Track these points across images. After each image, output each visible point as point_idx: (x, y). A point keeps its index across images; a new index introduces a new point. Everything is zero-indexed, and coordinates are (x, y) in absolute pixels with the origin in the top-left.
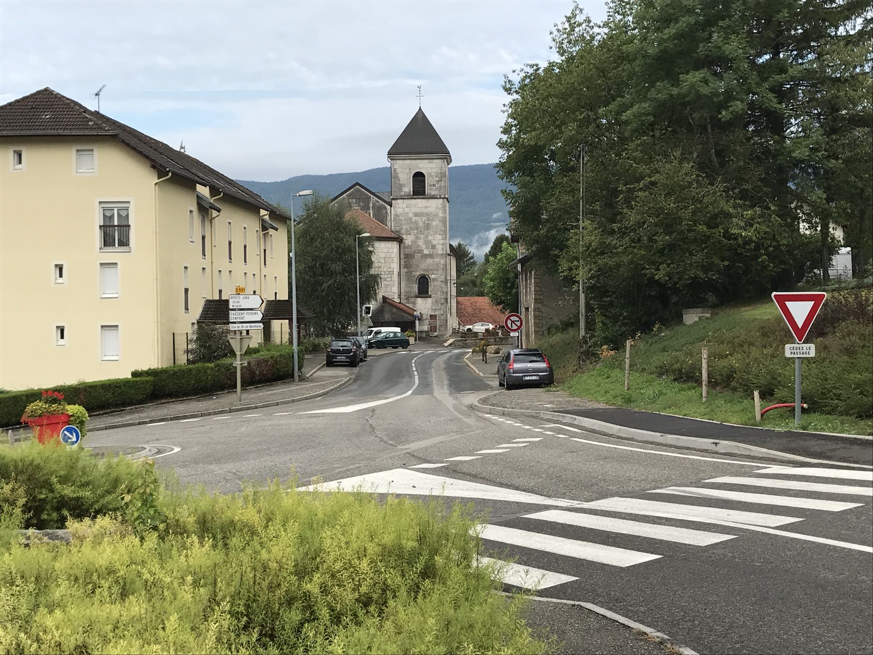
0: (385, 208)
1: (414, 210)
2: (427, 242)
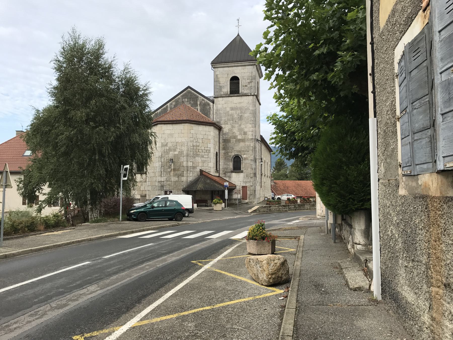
0: (209, 105)
2: (240, 130)
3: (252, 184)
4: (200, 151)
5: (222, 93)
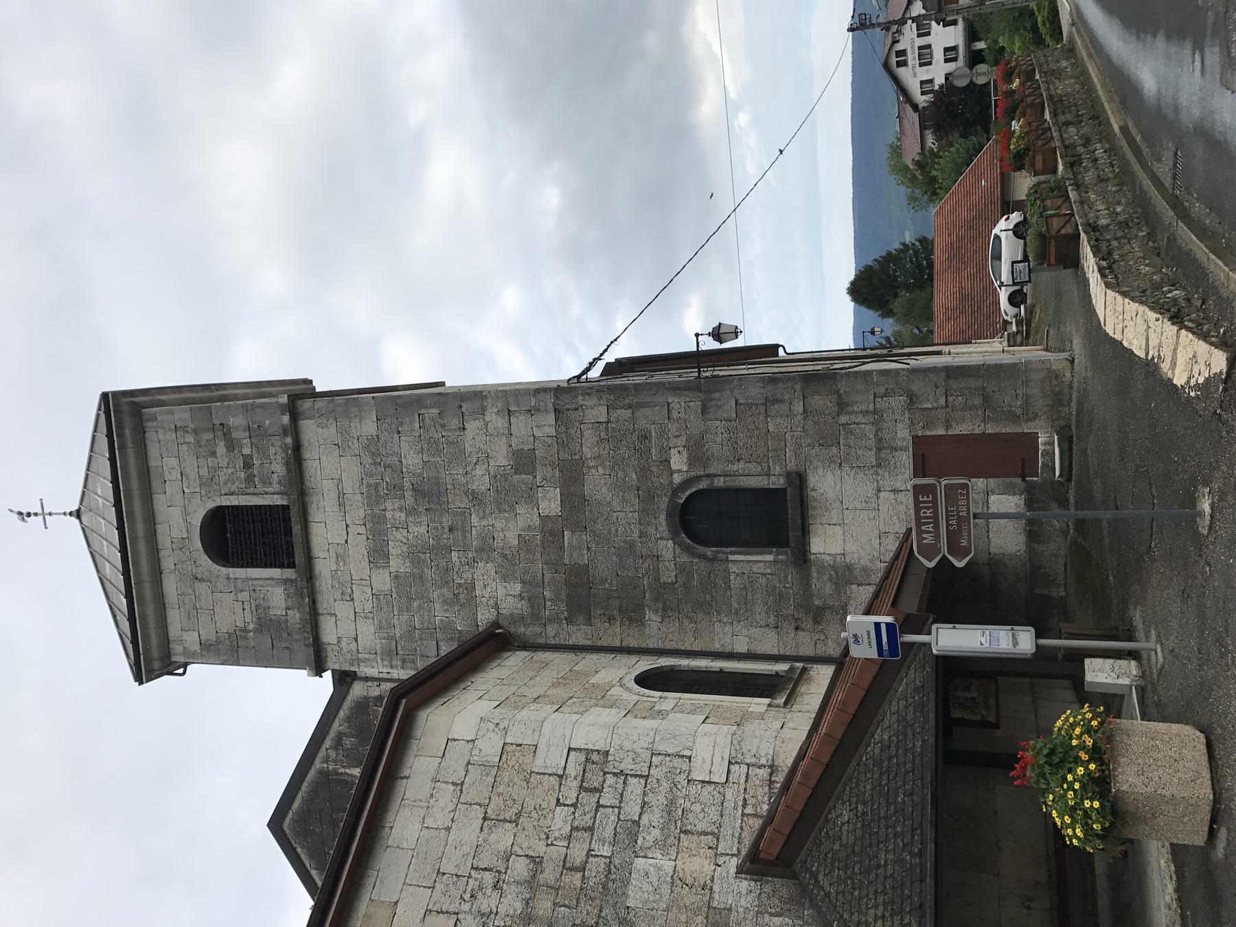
0: (363, 706)
1: (359, 565)
3: (899, 401)
4: (577, 854)
5: (295, 616)
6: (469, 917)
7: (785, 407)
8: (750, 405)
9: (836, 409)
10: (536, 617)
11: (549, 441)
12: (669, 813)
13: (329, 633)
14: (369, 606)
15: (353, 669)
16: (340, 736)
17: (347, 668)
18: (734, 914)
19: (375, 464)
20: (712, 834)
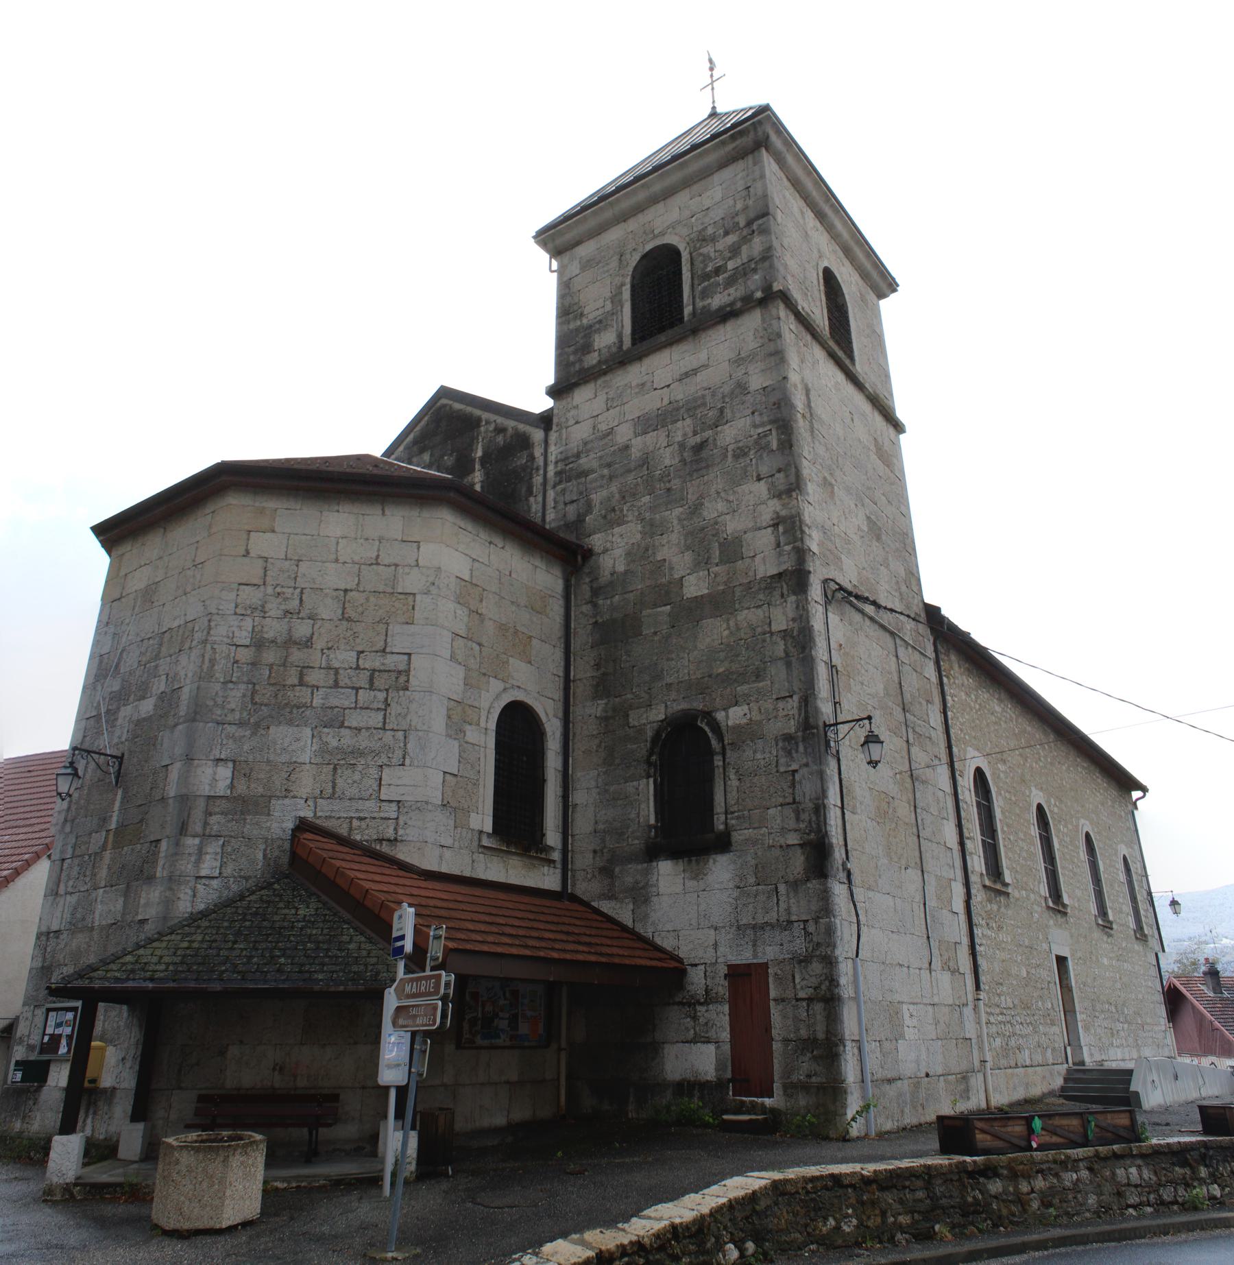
1: (639, 405)
4: (313, 677)
5: (592, 359)
6: (260, 595)
7: (792, 824)
8: (793, 785)
9: (791, 878)
10: (596, 592)
11: (751, 573)
12: (352, 752)
13: (582, 395)
14: (603, 427)
15: (554, 427)
16: (500, 430)
17: (555, 420)
18: (264, 818)
19: (723, 397)
20: (334, 793)
